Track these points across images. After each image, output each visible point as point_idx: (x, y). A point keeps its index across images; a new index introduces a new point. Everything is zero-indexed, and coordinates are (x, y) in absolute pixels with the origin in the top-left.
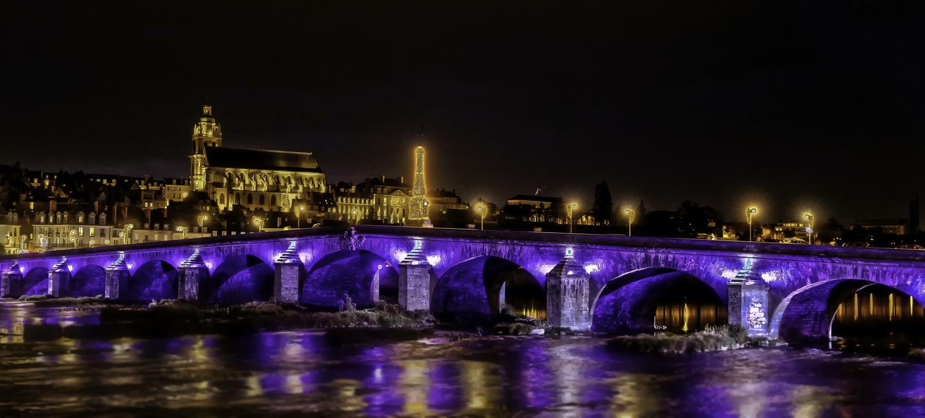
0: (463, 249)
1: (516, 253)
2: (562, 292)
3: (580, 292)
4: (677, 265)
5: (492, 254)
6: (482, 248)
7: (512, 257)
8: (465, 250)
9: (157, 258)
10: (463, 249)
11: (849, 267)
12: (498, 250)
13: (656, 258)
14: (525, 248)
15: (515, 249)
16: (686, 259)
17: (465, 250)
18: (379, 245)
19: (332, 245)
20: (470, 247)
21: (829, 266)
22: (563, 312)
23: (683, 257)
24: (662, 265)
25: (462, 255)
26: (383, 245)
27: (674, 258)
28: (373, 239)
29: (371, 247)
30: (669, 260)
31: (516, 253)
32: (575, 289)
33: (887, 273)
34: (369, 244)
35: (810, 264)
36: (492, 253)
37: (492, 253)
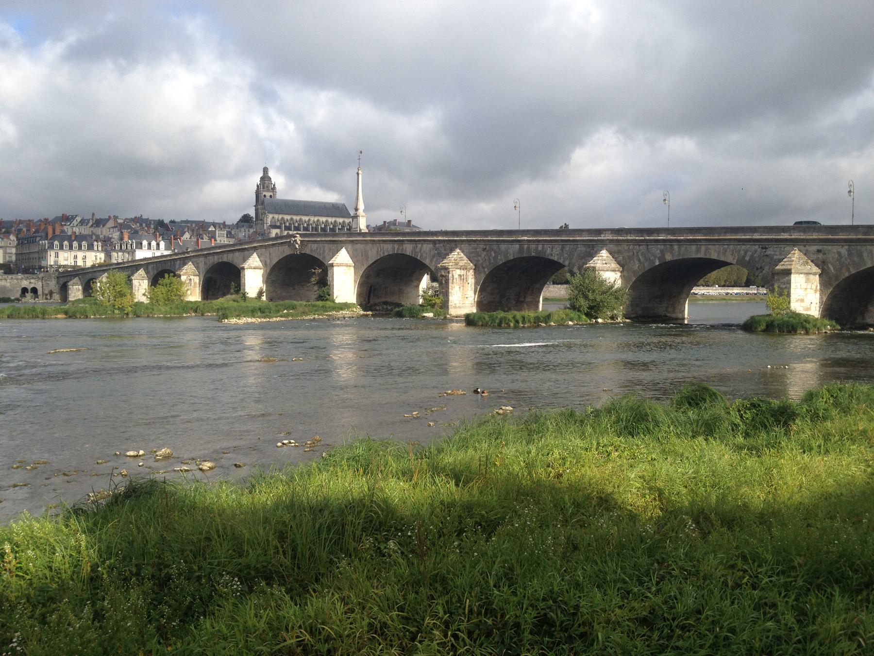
0: (378, 249)
1: (418, 250)
2: (450, 281)
3: (466, 281)
4: (545, 254)
5: (400, 252)
7: (415, 255)
10: (378, 249)
11: (694, 248)
12: (404, 249)
13: (528, 248)
14: (425, 246)
16: (553, 248)
18: (317, 249)
21: (676, 247)
22: (451, 298)
23: (551, 246)
24: (533, 254)
26: (320, 249)
27: (543, 248)
29: (311, 250)
30: (540, 249)
32: (462, 278)
33: (728, 250)
35: (659, 246)
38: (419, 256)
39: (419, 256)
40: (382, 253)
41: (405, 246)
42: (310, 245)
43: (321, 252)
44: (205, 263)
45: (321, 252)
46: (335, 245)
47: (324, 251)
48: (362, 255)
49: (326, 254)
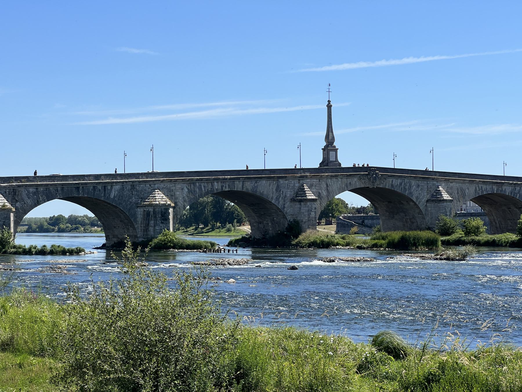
1: (516, 191)
5: (499, 192)
6: (491, 187)
7: (514, 195)
8: (478, 189)
9: (79, 194)
10: (476, 188)
12: (504, 190)
15: (516, 189)
17: (478, 189)
18: (401, 184)
19: (350, 183)
20: (482, 187)
25: (475, 193)
26: (405, 184)
28: (394, 180)
29: (392, 185)
31: (516, 191)
34: (391, 183)
36: (499, 191)
37: (499, 191)
38: (518, 196)
39: (518, 196)
40: (480, 192)
41: (504, 188)
42: (391, 180)
43: (407, 187)
44: (189, 191)
45: (407, 187)
46: (426, 182)
47: (410, 186)
48: (458, 193)
49: (412, 191)
